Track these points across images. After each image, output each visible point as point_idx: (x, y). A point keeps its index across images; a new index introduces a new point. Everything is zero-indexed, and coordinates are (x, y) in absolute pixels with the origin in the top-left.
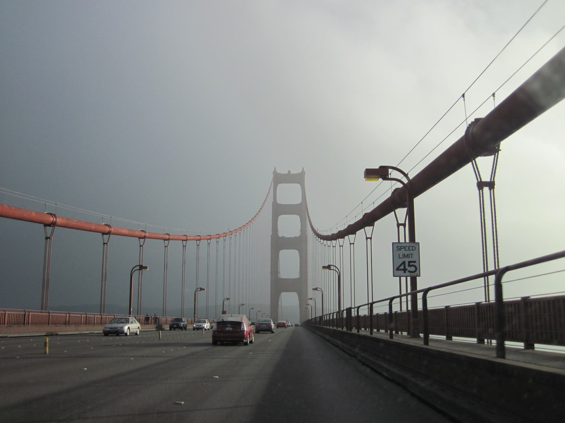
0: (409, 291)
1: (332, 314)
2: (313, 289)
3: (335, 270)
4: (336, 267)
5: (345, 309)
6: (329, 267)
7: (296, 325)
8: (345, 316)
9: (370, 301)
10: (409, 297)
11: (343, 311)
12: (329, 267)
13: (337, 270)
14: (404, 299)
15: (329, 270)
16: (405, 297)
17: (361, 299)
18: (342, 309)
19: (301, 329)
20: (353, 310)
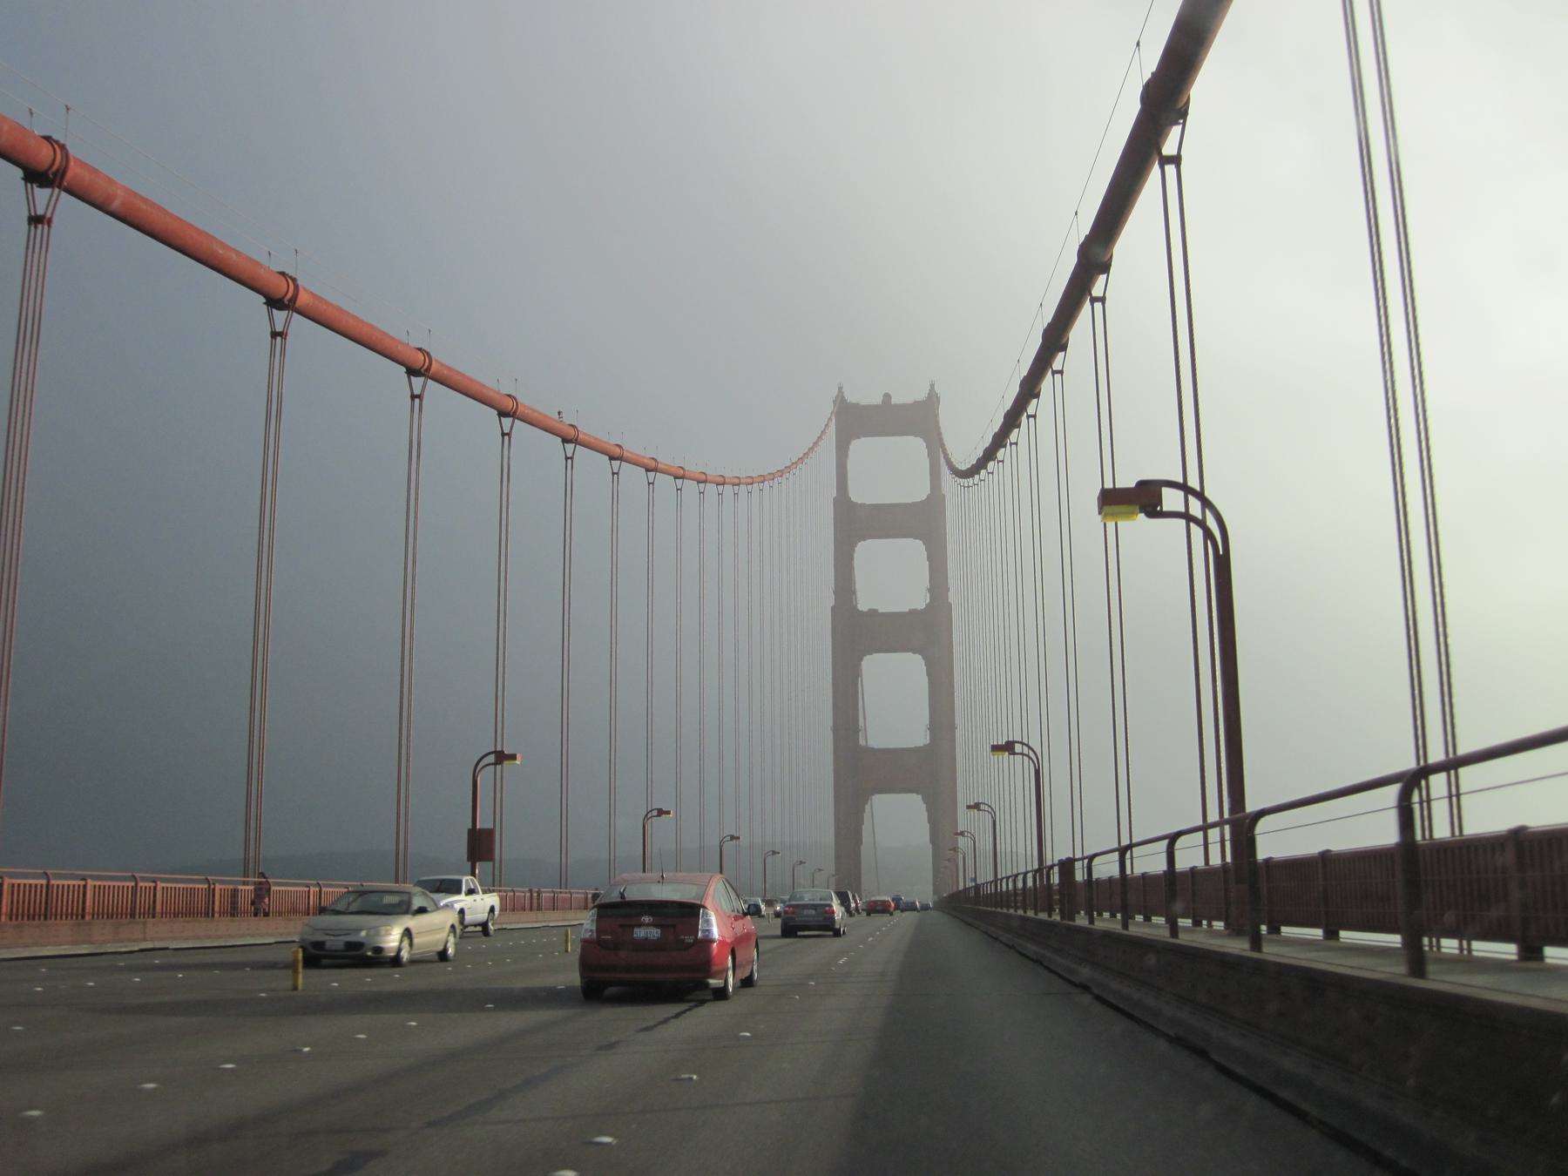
0: (1226, 815)
1: (1021, 877)
2: (969, 807)
3: (1028, 756)
4: (1030, 748)
5: (1056, 862)
6: (1009, 747)
7: (925, 908)
8: (1055, 879)
9: (1125, 842)
10: (1227, 828)
11: (1051, 867)
12: (1009, 747)
13: (1032, 754)
14: (1214, 834)
15: (1012, 757)
16: (1217, 830)
17: (1100, 836)
18: (1049, 863)
19: (934, 915)
20: (1078, 865)
